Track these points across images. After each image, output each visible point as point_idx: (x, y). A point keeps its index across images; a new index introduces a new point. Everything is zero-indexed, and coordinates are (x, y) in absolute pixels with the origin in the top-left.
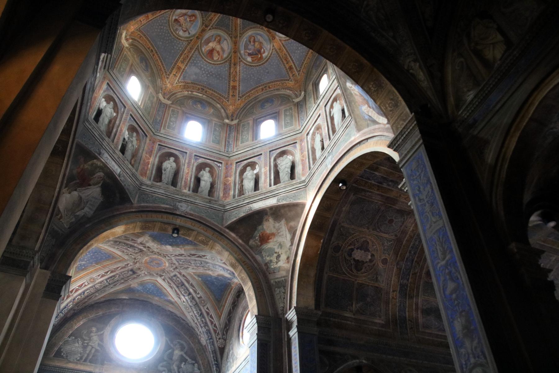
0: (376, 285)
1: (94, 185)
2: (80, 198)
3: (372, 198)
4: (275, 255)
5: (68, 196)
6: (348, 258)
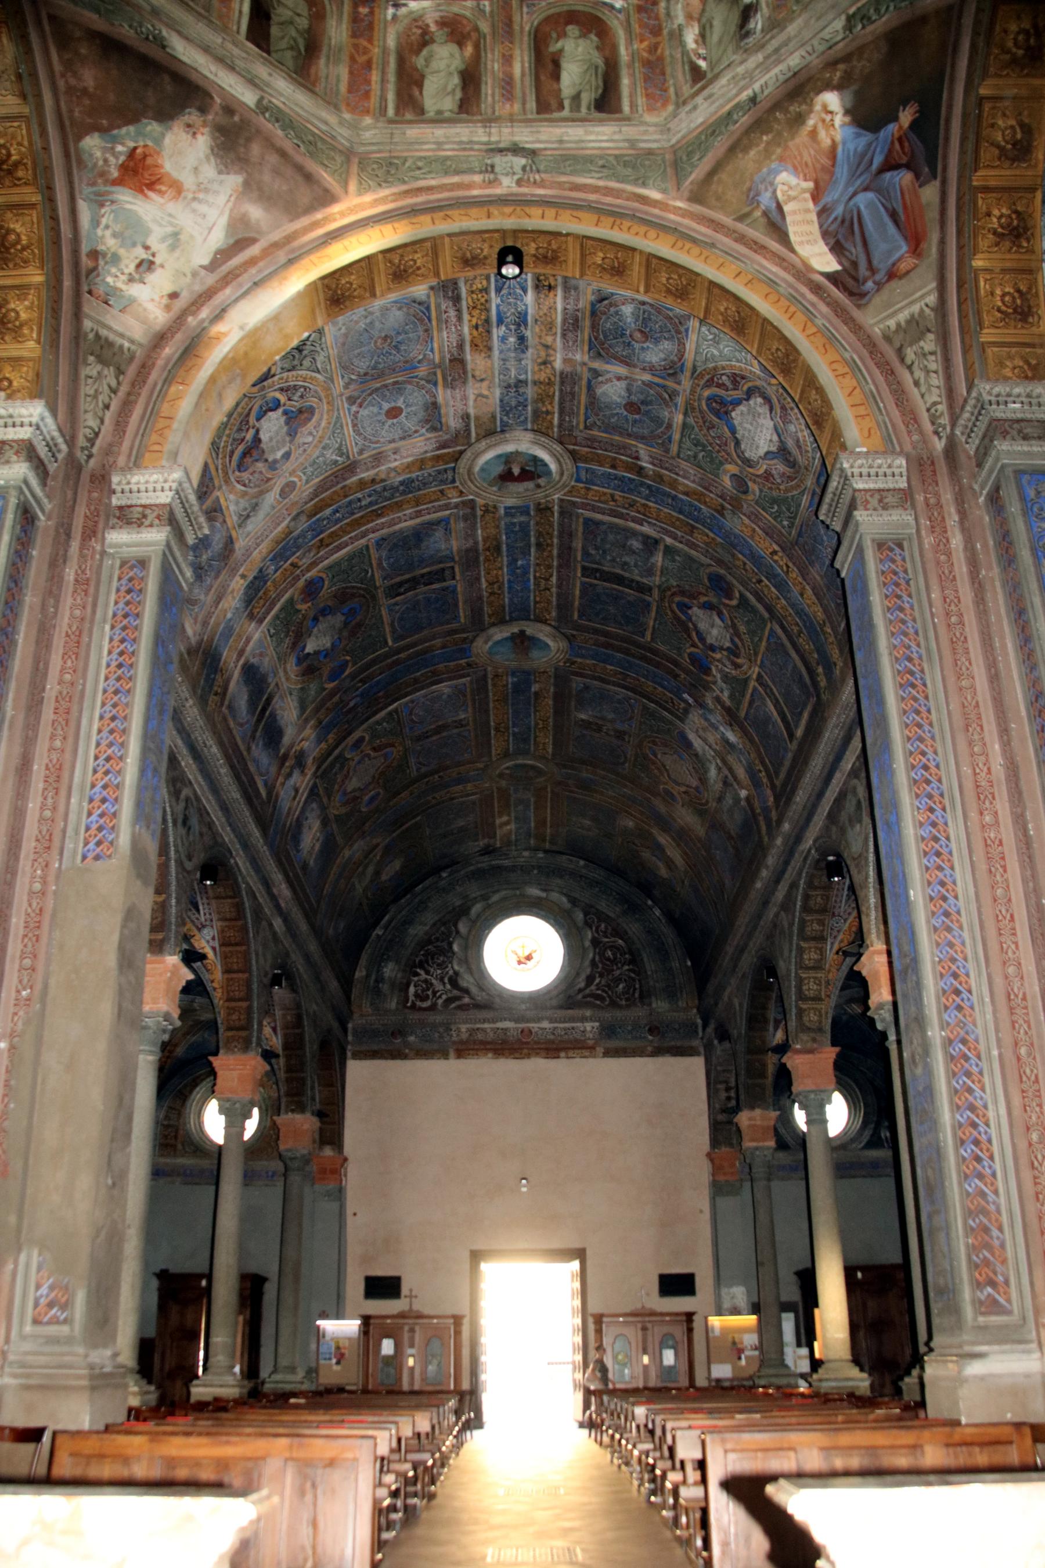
3: (440, 330)
4: (141, 254)
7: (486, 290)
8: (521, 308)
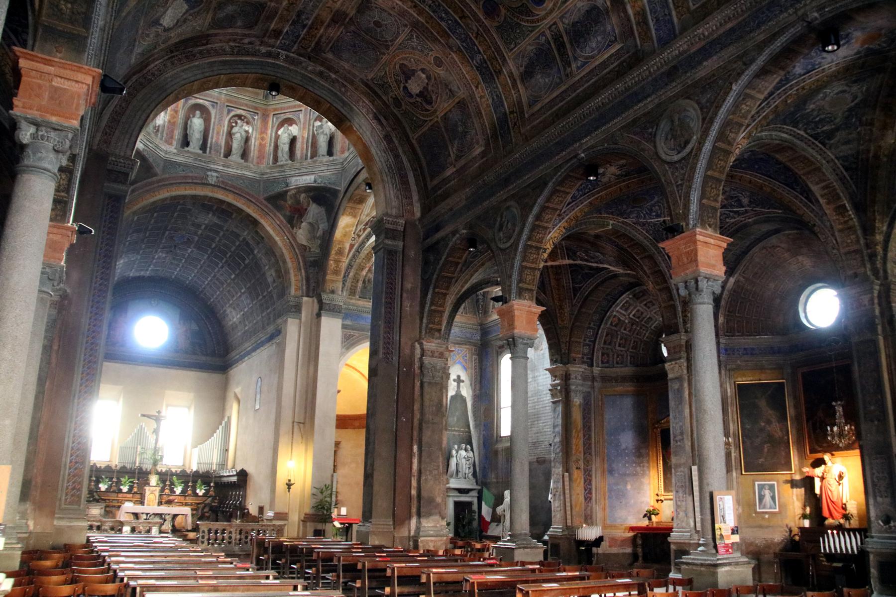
0: (457, 101)
1: (308, 205)
2: (310, 223)
5: (301, 231)
6: (412, 100)
7: (304, 38)
8: (292, 27)
